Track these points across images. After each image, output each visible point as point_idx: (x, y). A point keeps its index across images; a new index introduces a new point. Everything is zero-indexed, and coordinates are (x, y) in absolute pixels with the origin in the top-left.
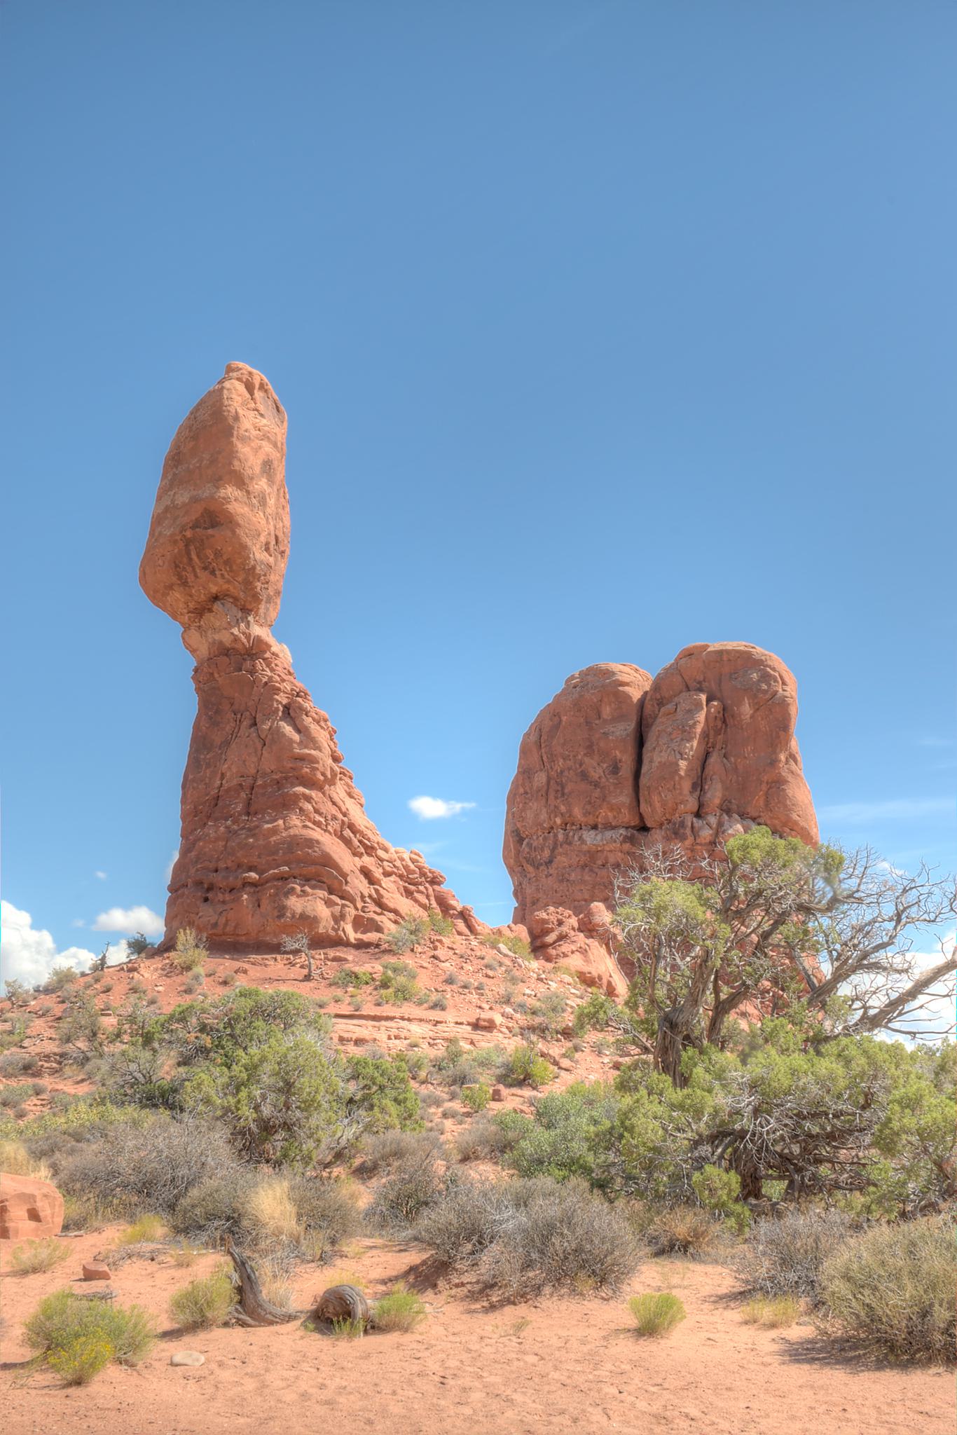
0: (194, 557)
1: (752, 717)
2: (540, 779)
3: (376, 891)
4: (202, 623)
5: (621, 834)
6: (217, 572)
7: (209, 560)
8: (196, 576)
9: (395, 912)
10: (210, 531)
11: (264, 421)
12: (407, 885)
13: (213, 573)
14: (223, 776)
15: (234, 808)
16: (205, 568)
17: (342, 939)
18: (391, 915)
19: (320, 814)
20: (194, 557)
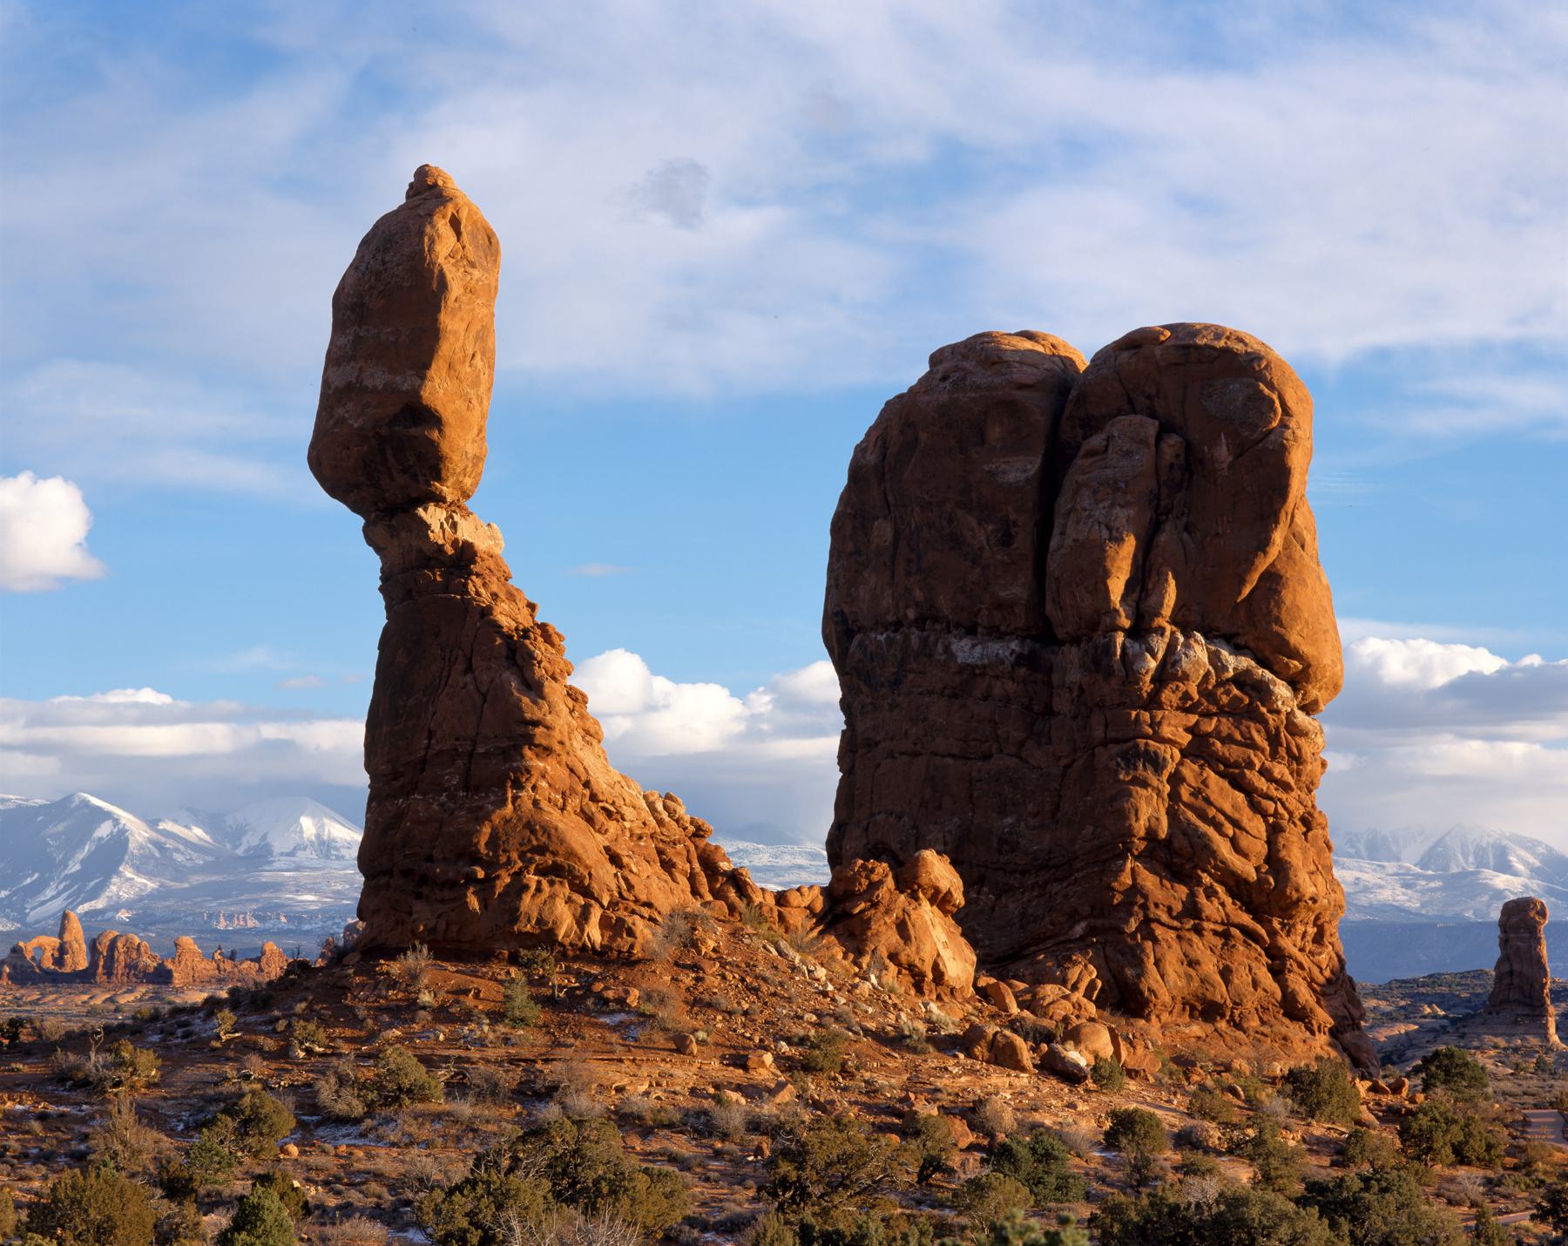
0: (391, 460)
1: (1230, 467)
2: (883, 532)
3: (626, 880)
4: (393, 522)
5: (1013, 652)
6: (420, 478)
7: (411, 463)
8: (392, 479)
9: (649, 905)
10: (413, 431)
11: (476, 273)
12: (661, 845)
13: (414, 477)
14: (431, 734)
15: (449, 781)
16: (404, 471)
17: (584, 945)
18: (646, 912)
19: (557, 791)
20: (391, 460)
